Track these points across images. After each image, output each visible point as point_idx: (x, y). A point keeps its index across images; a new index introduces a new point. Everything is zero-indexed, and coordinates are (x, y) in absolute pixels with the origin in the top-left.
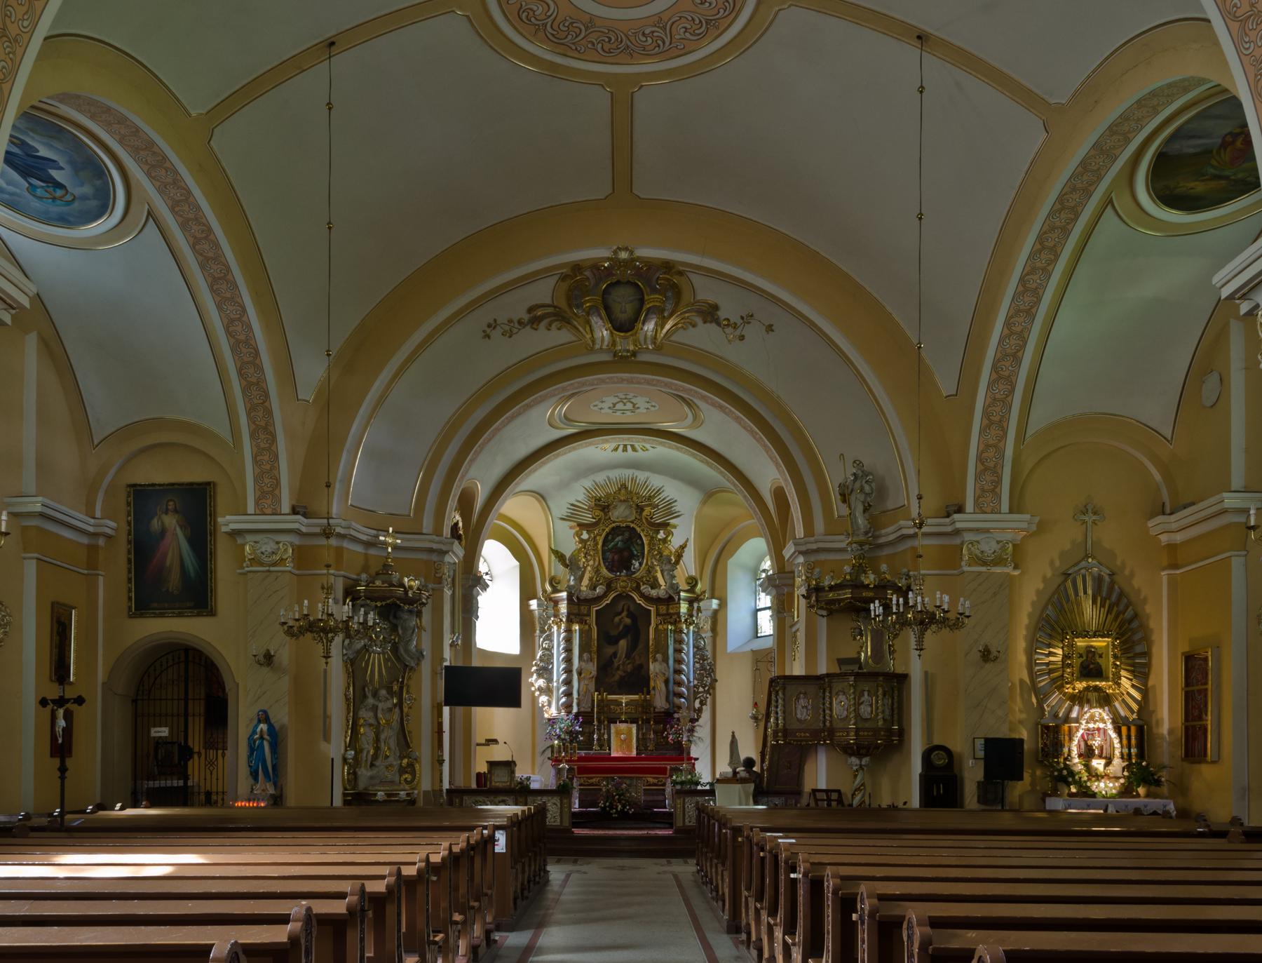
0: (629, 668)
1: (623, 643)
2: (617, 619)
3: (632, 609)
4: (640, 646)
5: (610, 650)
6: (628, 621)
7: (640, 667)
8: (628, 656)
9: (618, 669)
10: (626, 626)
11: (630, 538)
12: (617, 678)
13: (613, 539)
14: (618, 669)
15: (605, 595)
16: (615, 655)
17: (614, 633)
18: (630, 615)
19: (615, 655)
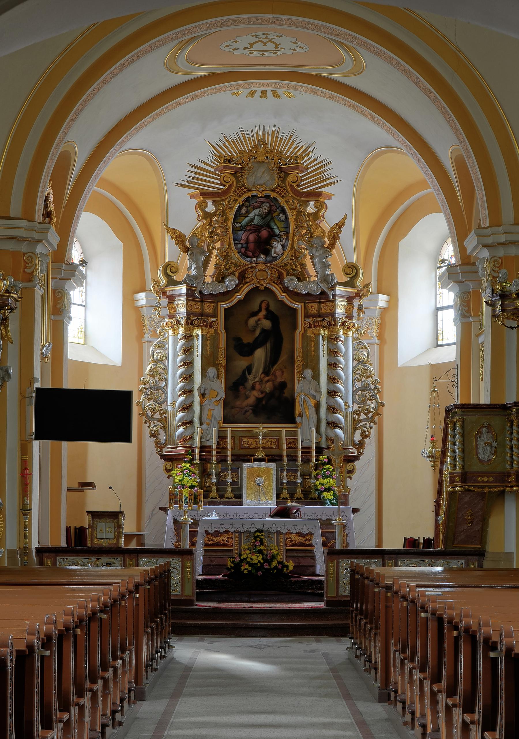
0: (268, 387)
1: (260, 354)
2: (252, 321)
3: (272, 307)
4: (284, 357)
5: (242, 363)
6: (267, 324)
7: (283, 385)
8: (266, 372)
9: (253, 388)
10: (263, 331)
11: (270, 212)
12: (251, 400)
13: (248, 212)
14: (253, 388)
15: (236, 289)
16: (249, 369)
17: (248, 339)
18: (271, 316)
19: (249, 369)
